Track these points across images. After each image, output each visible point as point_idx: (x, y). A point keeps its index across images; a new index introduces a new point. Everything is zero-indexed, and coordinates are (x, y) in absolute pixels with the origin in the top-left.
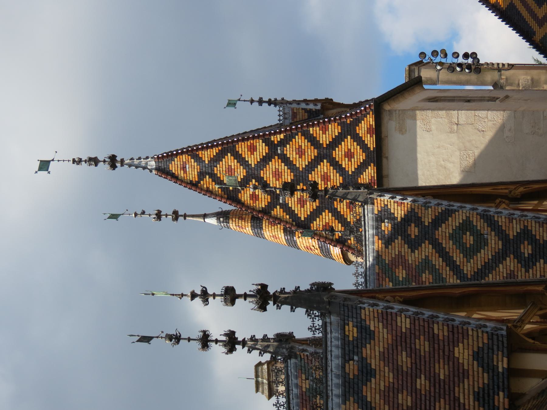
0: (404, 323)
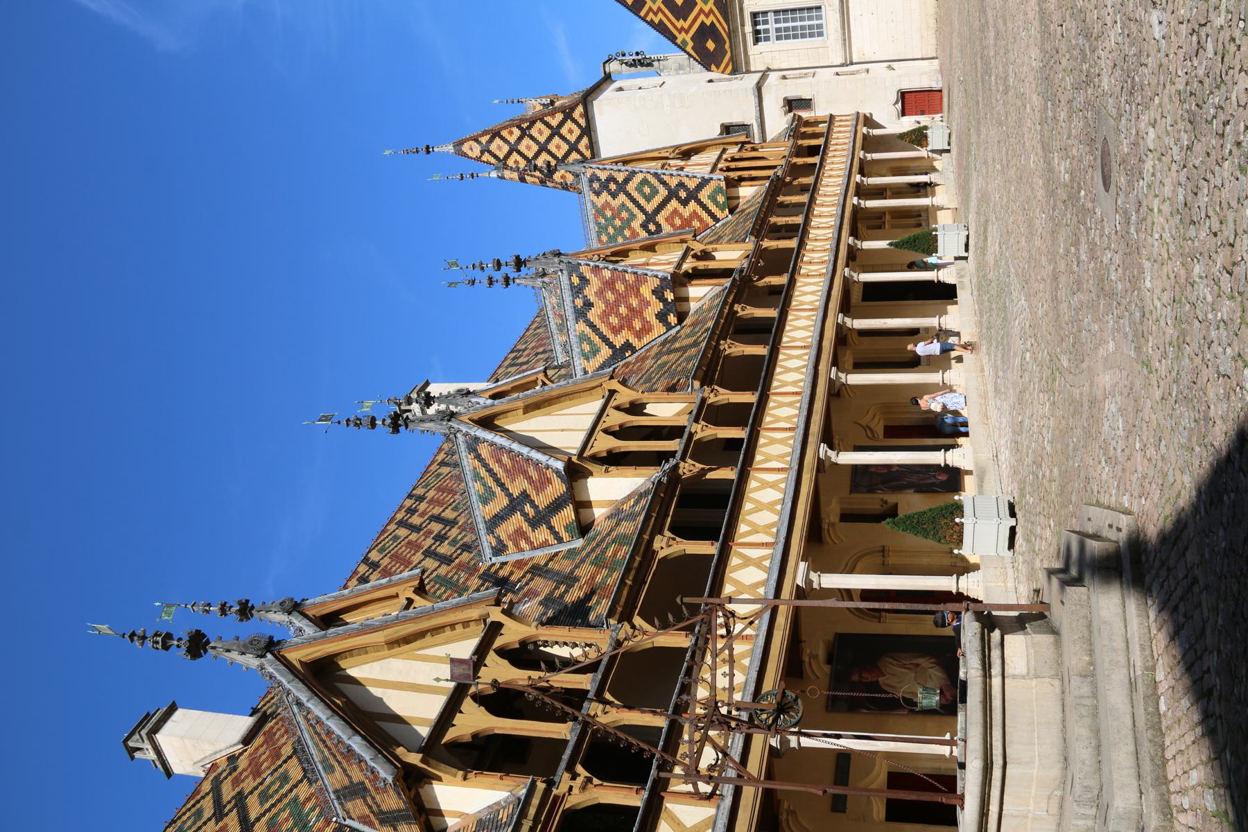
0: (607, 274)
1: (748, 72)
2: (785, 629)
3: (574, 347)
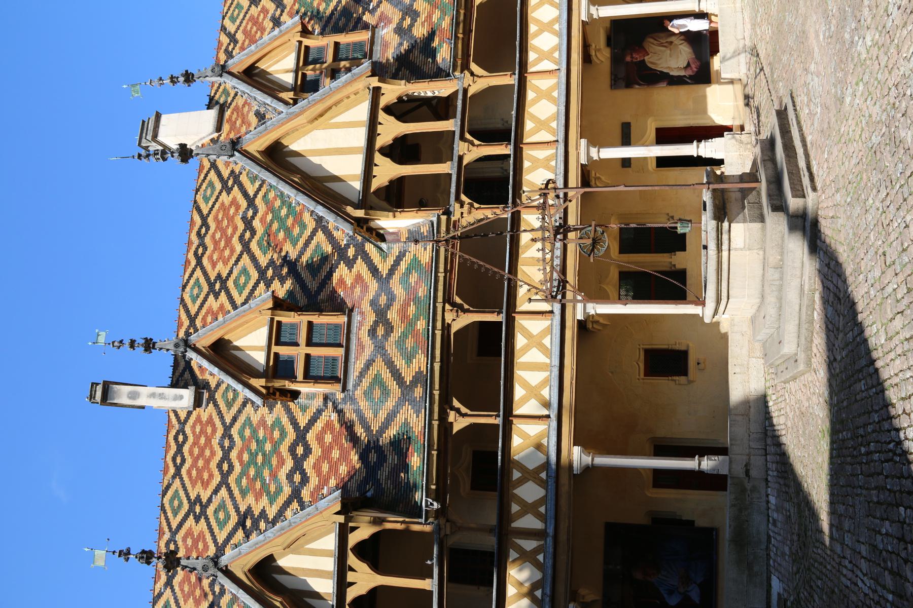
2: (578, 64)
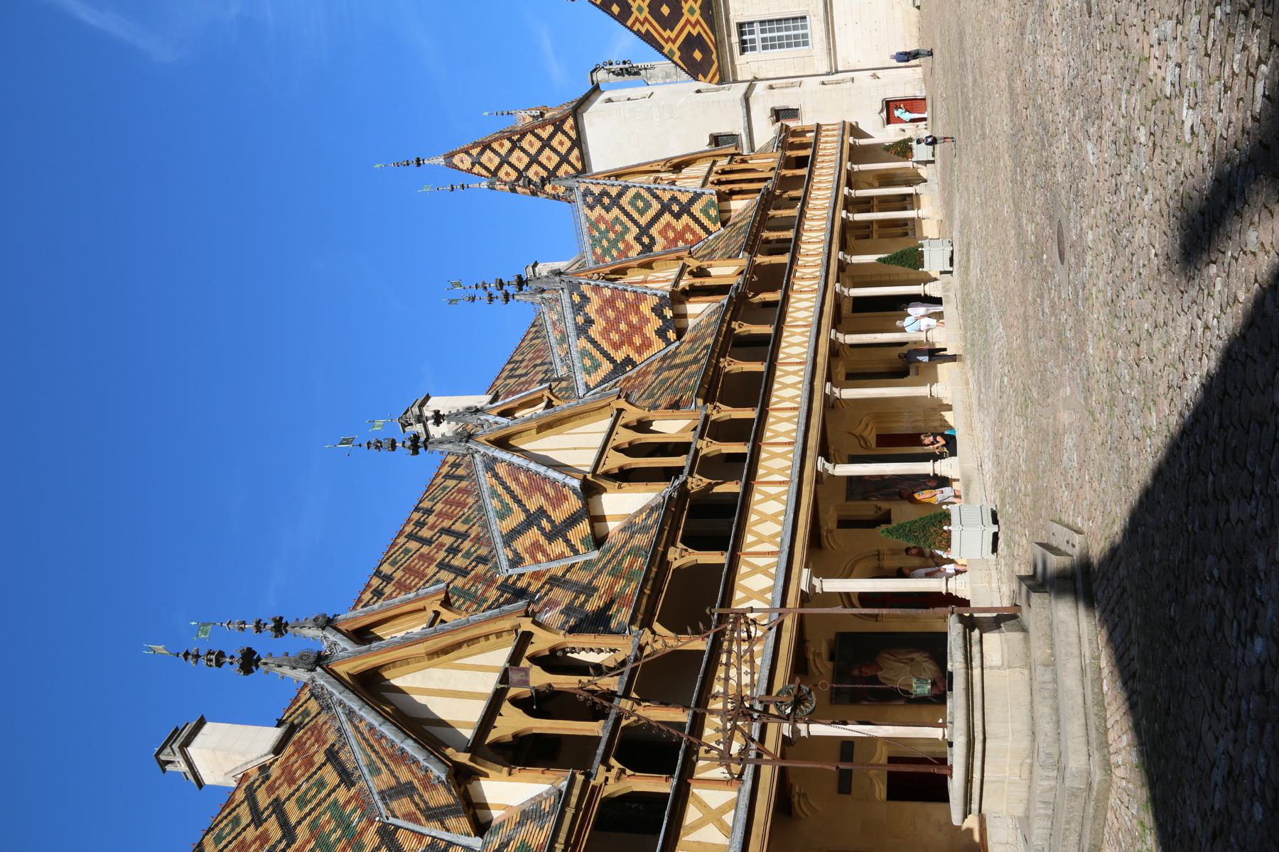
1: (735, 81)
3: (576, 362)
